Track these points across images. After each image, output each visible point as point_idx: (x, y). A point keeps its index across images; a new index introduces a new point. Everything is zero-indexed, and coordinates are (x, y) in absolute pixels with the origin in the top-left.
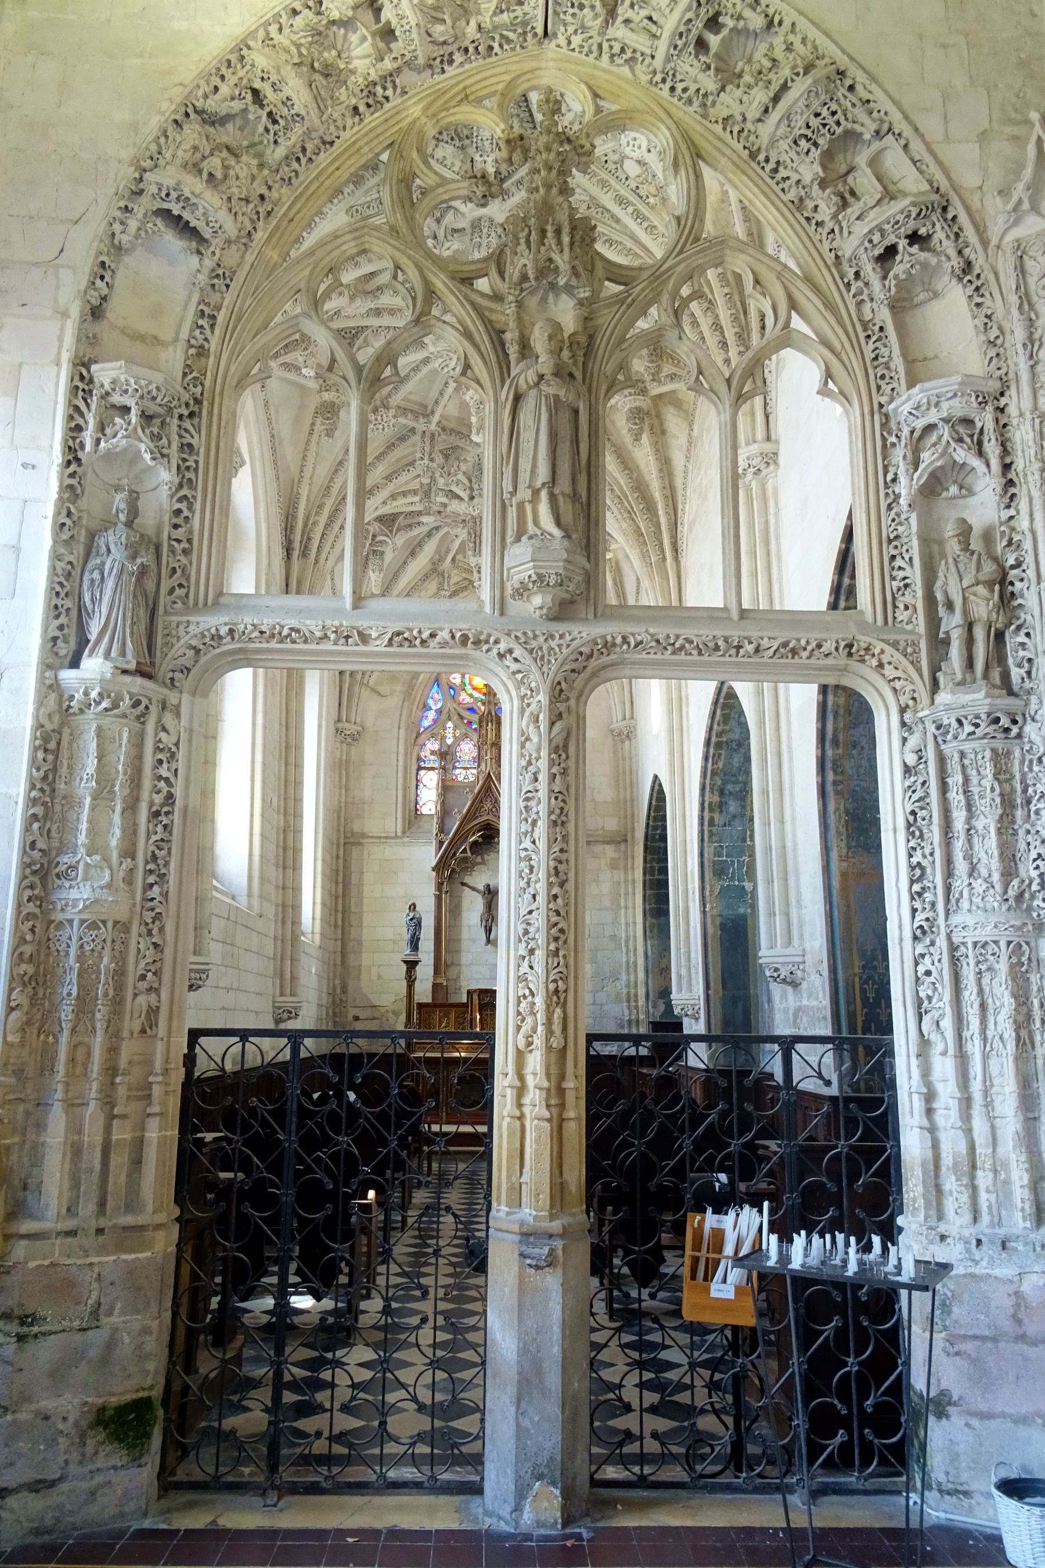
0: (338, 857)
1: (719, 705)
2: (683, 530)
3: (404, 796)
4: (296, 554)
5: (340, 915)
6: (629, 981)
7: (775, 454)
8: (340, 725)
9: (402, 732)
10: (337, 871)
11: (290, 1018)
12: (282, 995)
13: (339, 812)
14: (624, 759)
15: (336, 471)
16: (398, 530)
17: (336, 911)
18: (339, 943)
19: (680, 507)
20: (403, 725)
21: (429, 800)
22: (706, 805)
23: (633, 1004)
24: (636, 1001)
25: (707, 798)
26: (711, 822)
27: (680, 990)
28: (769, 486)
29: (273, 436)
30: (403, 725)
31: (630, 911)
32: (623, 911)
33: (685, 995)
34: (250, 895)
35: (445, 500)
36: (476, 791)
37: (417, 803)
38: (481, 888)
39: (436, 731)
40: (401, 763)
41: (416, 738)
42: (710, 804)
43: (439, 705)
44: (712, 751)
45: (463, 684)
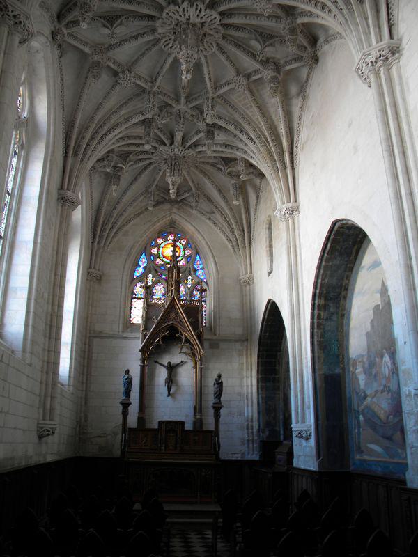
0: (85, 345)
1: (330, 240)
2: (297, 150)
3: (124, 312)
4: (71, 152)
5: (85, 377)
6: (248, 416)
7: (398, 48)
8: (90, 270)
9: (125, 278)
10: (85, 352)
11: (48, 435)
12: (44, 419)
13: (87, 318)
14: (246, 295)
15: (98, 108)
16: (130, 161)
17: (83, 374)
18: (84, 393)
19: (295, 137)
20: (126, 273)
21: (137, 315)
22: (316, 306)
23: (250, 431)
24: (252, 429)
25: (316, 302)
26: (319, 317)
27: (297, 422)
28: (394, 70)
29: (62, 80)
30: (126, 273)
31: (249, 379)
32: (245, 379)
33: (299, 425)
34: (24, 351)
35: (156, 145)
36: (166, 307)
37: (130, 317)
38: (166, 364)
39: (143, 277)
40: (123, 293)
41: (133, 281)
42: (319, 305)
43: (145, 265)
44: (322, 271)
45: (158, 253)
